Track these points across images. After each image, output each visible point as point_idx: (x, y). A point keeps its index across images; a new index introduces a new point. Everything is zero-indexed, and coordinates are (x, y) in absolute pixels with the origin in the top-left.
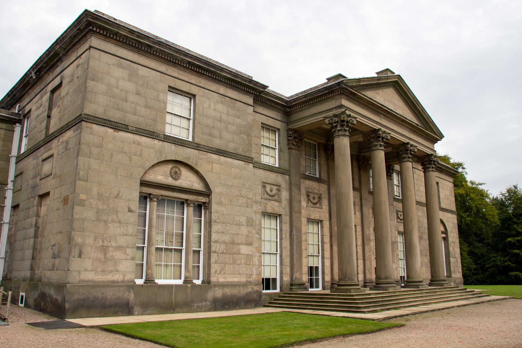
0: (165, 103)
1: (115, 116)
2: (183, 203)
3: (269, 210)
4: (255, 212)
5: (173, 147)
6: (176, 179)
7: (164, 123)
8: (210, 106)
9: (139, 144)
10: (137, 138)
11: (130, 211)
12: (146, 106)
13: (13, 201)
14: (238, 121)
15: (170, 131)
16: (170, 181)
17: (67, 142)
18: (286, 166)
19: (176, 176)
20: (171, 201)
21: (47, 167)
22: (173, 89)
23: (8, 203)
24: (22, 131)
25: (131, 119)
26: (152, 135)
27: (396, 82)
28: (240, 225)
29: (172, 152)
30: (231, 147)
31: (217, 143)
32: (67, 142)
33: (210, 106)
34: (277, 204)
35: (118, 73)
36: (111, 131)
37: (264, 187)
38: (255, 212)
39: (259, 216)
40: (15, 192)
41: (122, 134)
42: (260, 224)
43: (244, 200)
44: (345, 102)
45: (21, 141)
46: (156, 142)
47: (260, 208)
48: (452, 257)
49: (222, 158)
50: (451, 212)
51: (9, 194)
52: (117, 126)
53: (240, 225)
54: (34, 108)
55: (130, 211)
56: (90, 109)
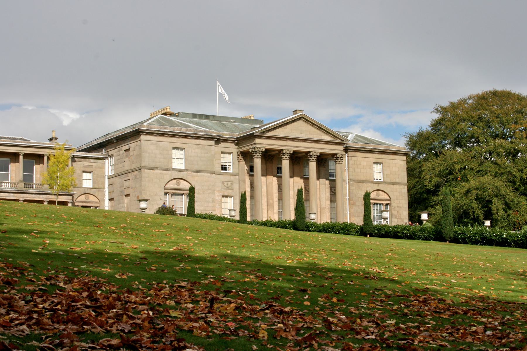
0: (171, 155)
1: (152, 165)
2: (182, 195)
3: (226, 194)
4: (218, 196)
5: (176, 173)
6: (178, 185)
7: (172, 163)
8: (192, 152)
9: (162, 174)
10: (162, 171)
11: (161, 200)
12: (164, 158)
13: (109, 196)
14: (206, 155)
15: (174, 167)
16: (176, 187)
17: (136, 176)
18: (237, 171)
19: (178, 184)
20: (177, 194)
21: (127, 184)
22: (174, 148)
23: (107, 198)
24: (108, 163)
25: (158, 164)
26: (167, 169)
27: (302, 117)
28: (209, 202)
29: (176, 175)
30: (202, 168)
31: (196, 167)
32: (136, 176)
33: (192, 152)
34: (230, 191)
35: (152, 147)
36: (151, 171)
37: (223, 183)
38: (218, 196)
39: (220, 198)
40: (110, 192)
41: (156, 171)
42: (221, 201)
43: (210, 191)
44: (257, 141)
45: (108, 168)
46: (169, 172)
47: (222, 194)
48: (396, 218)
49: (199, 173)
50: (399, 184)
51: (107, 193)
52: (153, 169)
53: (209, 202)
54: (115, 154)
55: (161, 200)
56: (143, 165)
